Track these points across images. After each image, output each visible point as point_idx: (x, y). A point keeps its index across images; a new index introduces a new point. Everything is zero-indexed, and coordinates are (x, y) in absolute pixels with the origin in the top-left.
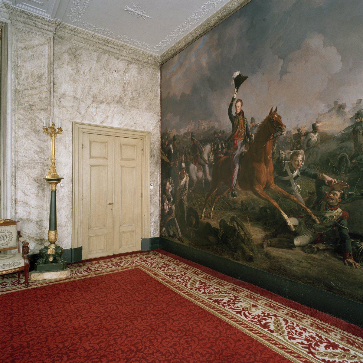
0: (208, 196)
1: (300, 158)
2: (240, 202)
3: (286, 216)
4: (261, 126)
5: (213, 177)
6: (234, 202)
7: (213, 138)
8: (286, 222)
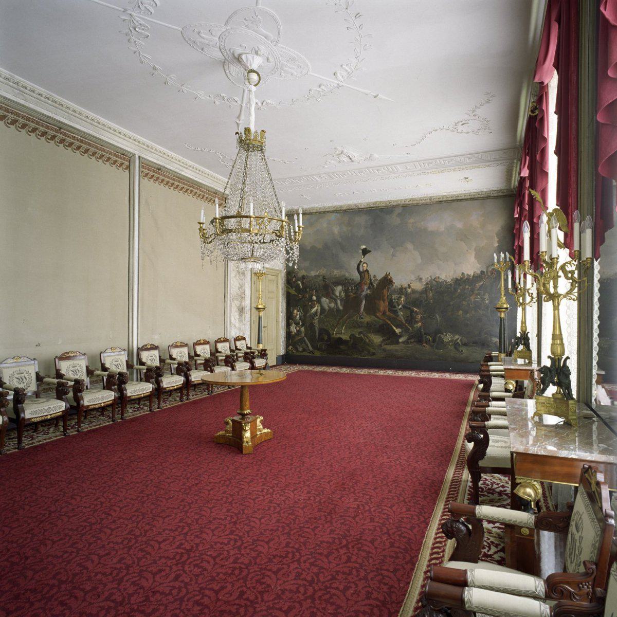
0: (339, 319)
1: (402, 299)
2: (366, 322)
3: (395, 328)
4: (380, 281)
5: (344, 307)
6: (361, 323)
7: (344, 282)
8: (395, 331)
